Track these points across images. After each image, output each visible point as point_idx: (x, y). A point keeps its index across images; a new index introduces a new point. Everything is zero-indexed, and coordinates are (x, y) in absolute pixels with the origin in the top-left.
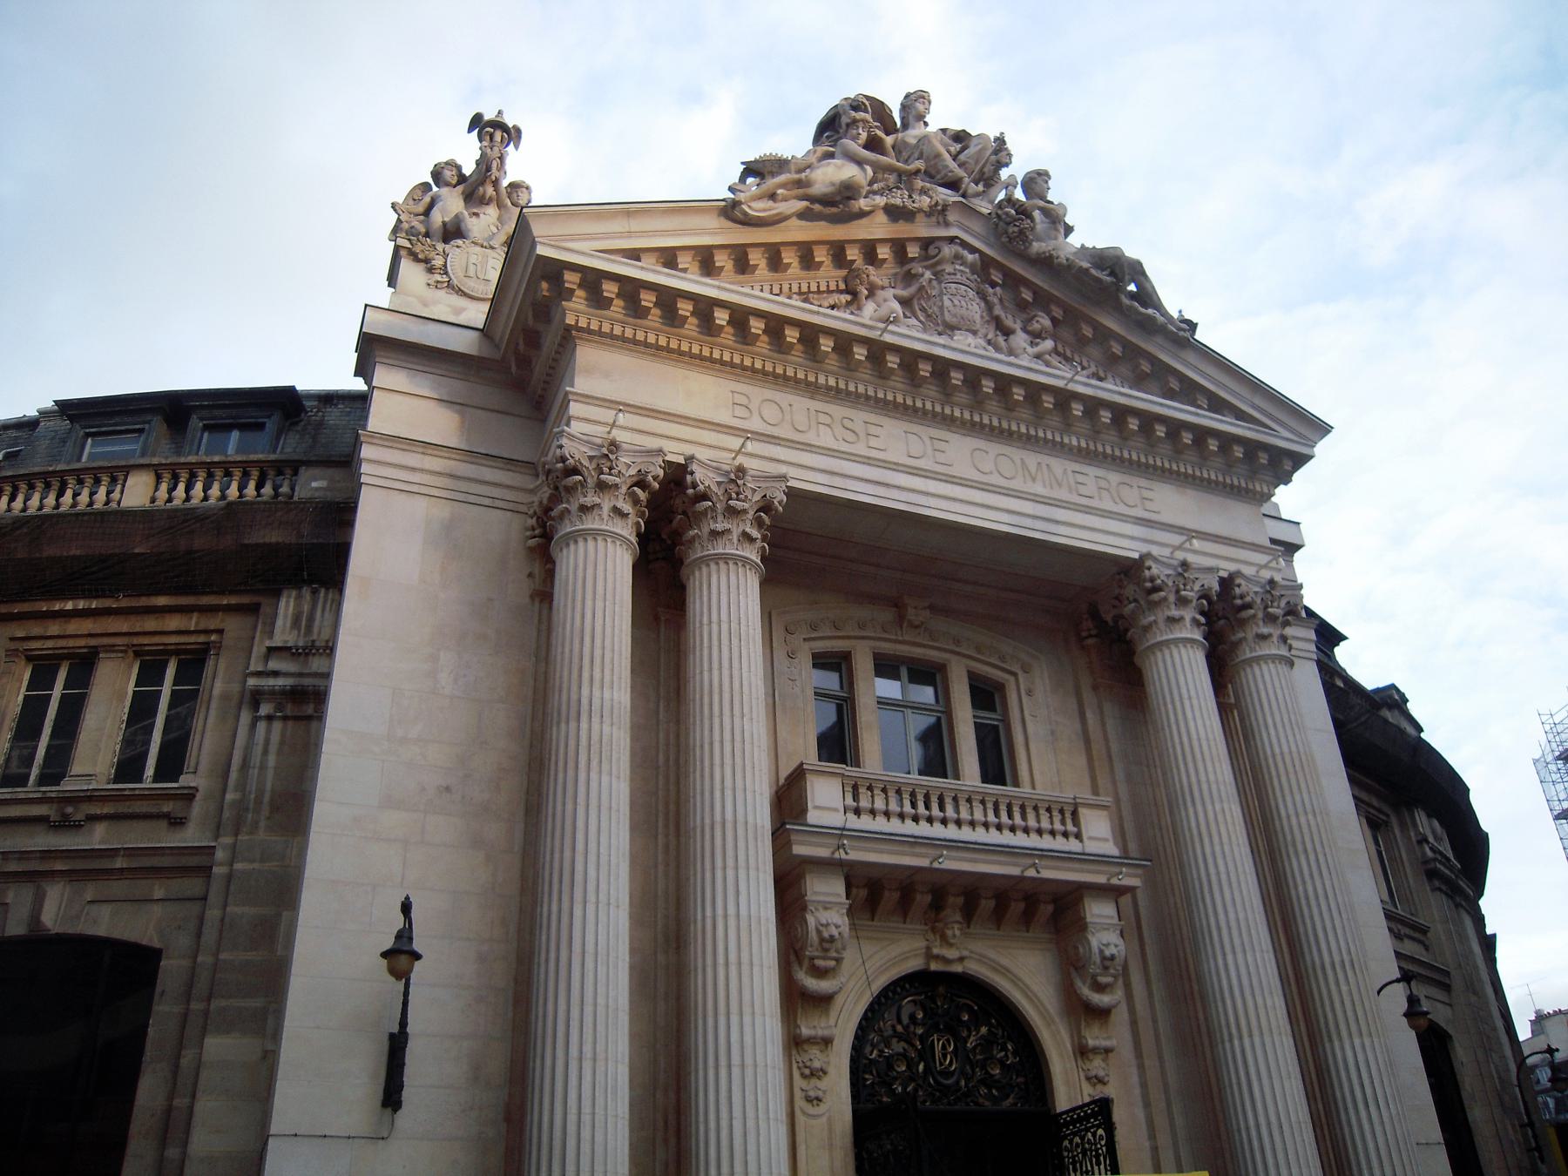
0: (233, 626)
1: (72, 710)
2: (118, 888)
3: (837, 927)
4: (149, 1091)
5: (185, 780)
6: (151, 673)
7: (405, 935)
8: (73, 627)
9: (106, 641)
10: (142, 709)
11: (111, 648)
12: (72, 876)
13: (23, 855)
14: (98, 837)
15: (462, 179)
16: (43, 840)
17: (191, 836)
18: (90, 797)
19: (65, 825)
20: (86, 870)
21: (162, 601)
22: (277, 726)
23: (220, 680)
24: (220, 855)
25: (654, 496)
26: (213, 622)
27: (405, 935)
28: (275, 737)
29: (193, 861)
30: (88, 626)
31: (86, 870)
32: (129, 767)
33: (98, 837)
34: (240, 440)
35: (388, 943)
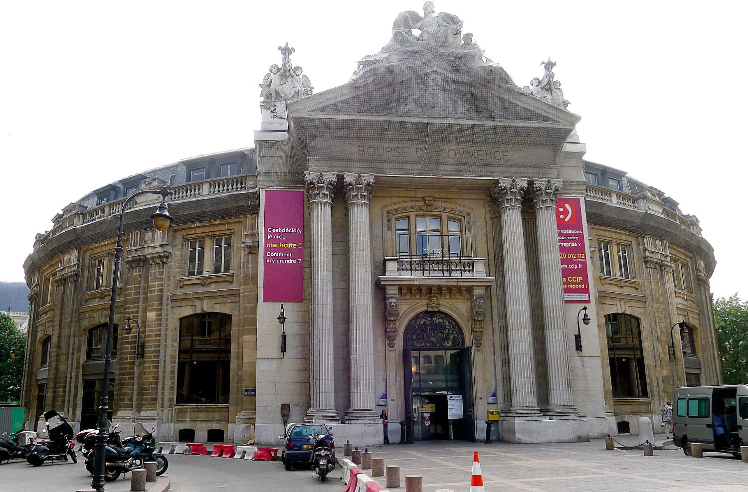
0: (236, 227)
1: (202, 253)
2: (220, 300)
3: (394, 302)
4: (233, 348)
5: (231, 272)
6: (219, 242)
7: (283, 314)
8: (198, 231)
9: (207, 234)
10: (218, 252)
11: (207, 236)
12: (210, 298)
13: (197, 294)
14: (213, 288)
15: (279, 70)
16: (201, 289)
17: (234, 286)
18: (210, 277)
19: (204, 285)
20: (212, 296)
21: (217, 222)
22: (250, 256)
23: (235, 244)
24: (241, 291)
25: (335, 187)
26: (232, 227)
27: (283, 314)
28: (250, 259)
29: (235, 293)
30: (201, 230)
31: (212, 296)
32: (217, 270)
33: (213, 288)
34: (231, 167)
35: (279, 315)
